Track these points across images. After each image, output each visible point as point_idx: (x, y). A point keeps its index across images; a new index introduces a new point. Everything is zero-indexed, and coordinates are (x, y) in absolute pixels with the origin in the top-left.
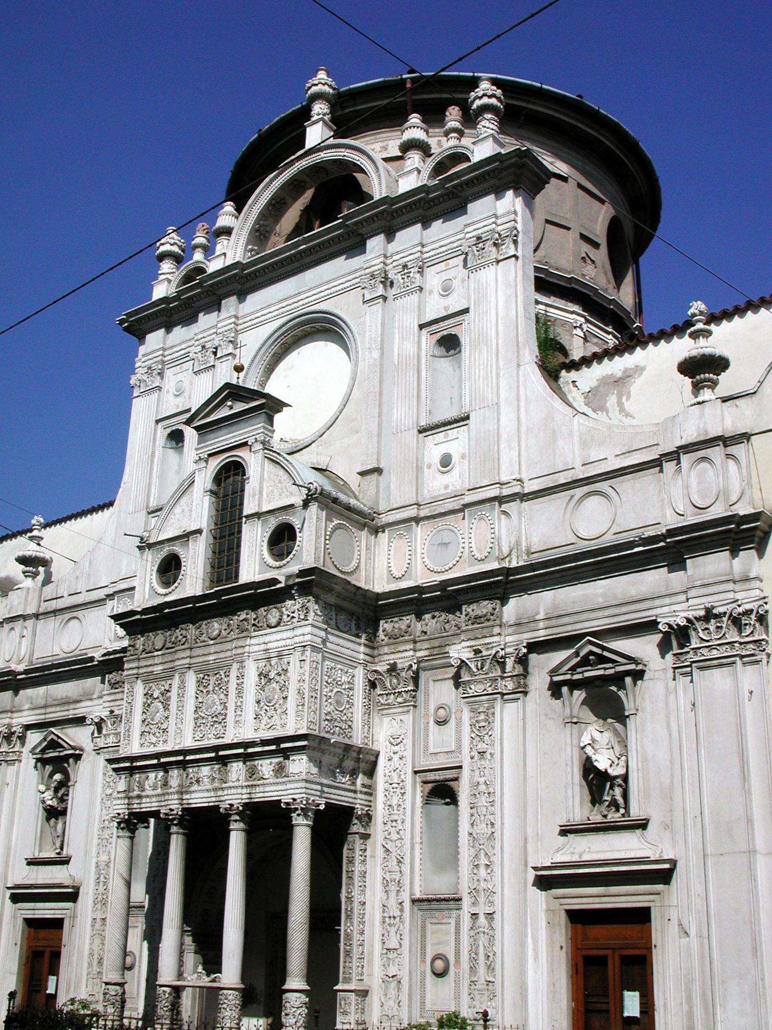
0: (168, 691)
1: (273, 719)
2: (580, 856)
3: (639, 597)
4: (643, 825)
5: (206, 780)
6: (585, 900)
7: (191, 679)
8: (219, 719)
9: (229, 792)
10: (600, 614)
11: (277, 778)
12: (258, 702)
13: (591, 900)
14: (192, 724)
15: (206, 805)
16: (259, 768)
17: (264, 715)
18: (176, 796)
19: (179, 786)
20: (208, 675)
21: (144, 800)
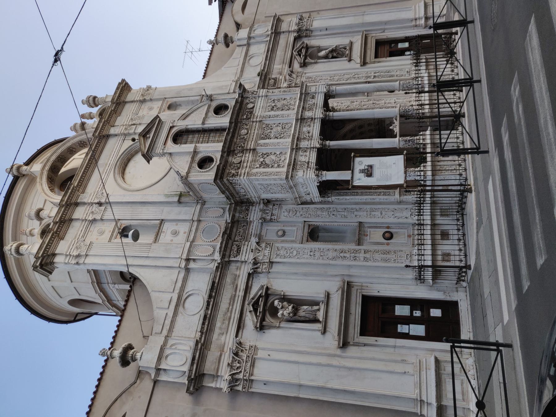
0: (263, 153)
5: (309, 129)
12: (282, 110)
15: (320, 125)
16: (310, 105)
18: (313, 141)
19: (308, 141)
21: (310, 161)
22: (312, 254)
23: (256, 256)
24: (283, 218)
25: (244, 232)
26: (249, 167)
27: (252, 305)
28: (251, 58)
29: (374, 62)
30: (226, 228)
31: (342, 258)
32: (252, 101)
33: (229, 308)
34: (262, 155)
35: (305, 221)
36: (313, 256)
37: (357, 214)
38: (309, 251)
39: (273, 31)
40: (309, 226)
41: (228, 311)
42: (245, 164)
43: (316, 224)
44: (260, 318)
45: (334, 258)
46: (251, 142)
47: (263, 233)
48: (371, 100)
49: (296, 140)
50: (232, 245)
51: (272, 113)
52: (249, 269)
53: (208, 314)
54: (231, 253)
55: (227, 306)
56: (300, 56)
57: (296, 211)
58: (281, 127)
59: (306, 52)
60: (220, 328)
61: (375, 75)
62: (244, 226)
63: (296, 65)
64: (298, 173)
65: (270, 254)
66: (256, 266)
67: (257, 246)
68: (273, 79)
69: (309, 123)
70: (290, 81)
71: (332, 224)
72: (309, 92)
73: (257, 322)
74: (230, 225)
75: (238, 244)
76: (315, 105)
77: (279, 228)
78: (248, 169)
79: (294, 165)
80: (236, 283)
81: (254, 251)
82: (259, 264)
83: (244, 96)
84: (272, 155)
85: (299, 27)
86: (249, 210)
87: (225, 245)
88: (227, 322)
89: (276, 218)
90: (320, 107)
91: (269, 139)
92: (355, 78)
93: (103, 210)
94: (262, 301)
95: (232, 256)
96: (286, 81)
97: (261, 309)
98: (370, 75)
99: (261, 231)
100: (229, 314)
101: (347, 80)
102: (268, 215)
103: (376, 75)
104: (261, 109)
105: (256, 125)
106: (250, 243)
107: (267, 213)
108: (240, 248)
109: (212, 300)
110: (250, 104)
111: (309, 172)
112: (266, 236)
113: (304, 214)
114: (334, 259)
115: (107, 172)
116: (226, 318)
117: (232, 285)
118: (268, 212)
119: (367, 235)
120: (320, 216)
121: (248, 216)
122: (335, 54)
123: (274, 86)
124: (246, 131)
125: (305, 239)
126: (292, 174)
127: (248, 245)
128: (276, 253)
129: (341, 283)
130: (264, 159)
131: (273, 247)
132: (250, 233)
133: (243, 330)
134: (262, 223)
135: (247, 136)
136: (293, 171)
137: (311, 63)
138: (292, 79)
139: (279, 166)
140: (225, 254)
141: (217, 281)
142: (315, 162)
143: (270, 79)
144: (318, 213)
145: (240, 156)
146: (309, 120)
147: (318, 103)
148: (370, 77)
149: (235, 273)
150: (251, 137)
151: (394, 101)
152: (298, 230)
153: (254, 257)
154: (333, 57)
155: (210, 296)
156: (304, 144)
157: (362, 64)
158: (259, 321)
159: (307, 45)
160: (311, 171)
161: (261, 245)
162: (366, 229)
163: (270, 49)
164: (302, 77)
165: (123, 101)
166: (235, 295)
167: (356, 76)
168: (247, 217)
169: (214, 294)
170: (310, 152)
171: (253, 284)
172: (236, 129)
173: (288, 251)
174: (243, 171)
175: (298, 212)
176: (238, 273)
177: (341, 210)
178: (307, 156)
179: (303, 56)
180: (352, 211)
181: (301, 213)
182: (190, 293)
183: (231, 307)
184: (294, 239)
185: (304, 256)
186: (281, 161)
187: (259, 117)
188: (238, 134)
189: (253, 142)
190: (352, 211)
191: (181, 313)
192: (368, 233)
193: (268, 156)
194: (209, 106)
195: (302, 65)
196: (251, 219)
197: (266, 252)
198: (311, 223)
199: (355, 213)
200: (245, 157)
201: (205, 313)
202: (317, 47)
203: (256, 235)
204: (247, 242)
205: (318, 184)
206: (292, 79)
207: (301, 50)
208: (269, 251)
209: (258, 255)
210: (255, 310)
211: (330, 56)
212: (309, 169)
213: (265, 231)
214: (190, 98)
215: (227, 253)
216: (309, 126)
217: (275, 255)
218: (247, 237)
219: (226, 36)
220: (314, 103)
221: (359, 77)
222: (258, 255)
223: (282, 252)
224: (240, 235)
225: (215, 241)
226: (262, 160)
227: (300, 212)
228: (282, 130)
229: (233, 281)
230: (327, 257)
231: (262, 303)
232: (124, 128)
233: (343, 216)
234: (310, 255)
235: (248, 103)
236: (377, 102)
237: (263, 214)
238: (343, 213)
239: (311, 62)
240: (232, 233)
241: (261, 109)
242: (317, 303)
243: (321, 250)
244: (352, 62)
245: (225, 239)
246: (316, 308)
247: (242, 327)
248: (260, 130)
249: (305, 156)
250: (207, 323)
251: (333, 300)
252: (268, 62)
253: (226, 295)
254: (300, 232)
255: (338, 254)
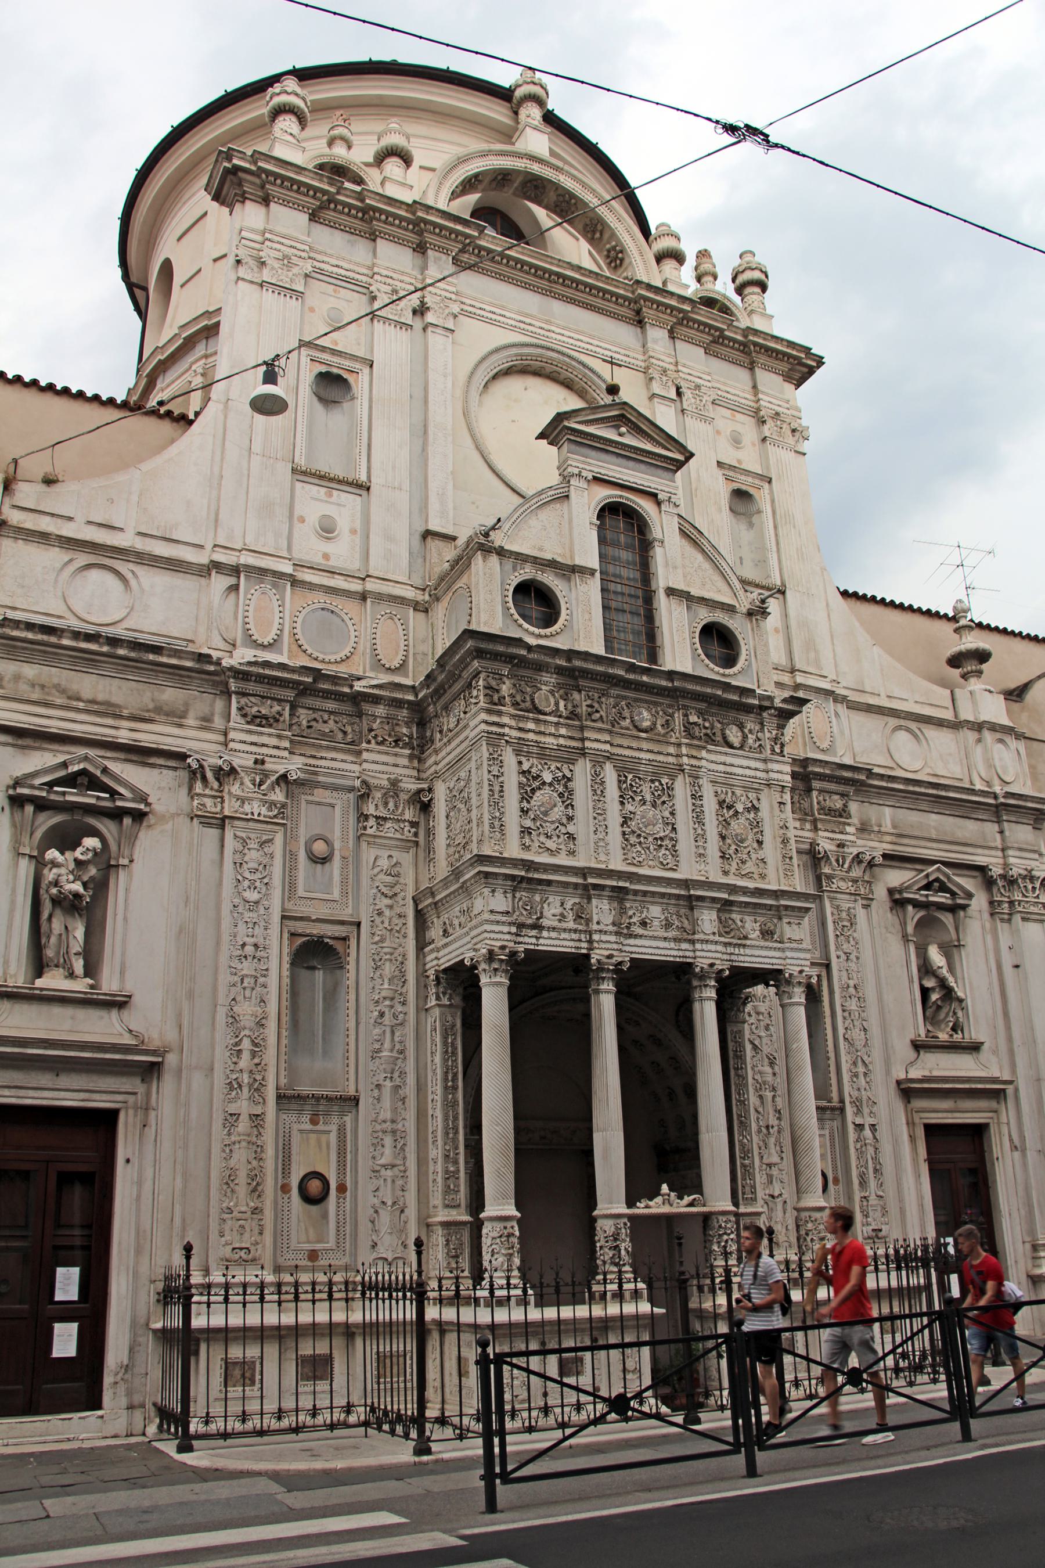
0: (569, 780)
1: (748, 864)
2: (930, 1071)
3: (963, 841)
4: (975, 1048)
5: (656, 923)
6: (940, 1115)
7: (610, 774)
8: (667, 842)
9: (705, 947)
10: (935, 845)
11: (766, 940)
12: (723, 838)
13: (945, 1115)
14: (619, 838)
15: (672, 959)
16: (739, 923)
17: (734, 856)
18: (613, 938)
19: (614, 924)
20: (640, 778)
21: (545, 934)
22: (249, 949)
23: (242, 774)
24: (369, 854)
25: (324, 734)
26: (520, 738)
27: (84, 769)
28: (916, 736)
29: (910, 1124)
30: (334, 679)
31: (237, 1044)
32: (750, 741)
33: (79, 699)
34: (564, 776)
35: (359, 924)
36: (239, 952)
37: (383, 1090)
38: (260, 941)
39: (1002, 800)
40: (345, 939)
41: (69, 698)
42: (531, 726)
43: (352, 959)
44: (44, 794)
45: (234, 1019)
46: (606, 742)
47: (320, 795)
48: (779, 1119)
49: (614, 883)
50: (280, 701)
51: (710, 805)
52: (198, 756)
53: (60, 637)
54: (252, 699)
55: (87, 694)
56: (928, 887)
57: (396, 894)
58: (662, 834)
59: (940, 907)
60: (17, 678)
61: (867, 1127)
62: (345, 733)
63: (896, 877)
64: (499, 894)
65: (249, 816)
66: (209, 775)
67: (273, 778)
68: (845, 806)
69: (677, 923)
70: (837, 861)
71: (352, 1012)
72: (785, 920)
73: (33, 787)
74: (347, 690)
75: (282, 719)
76: (739, 942)
77: (337, 845)
78: (515, 733)
79: (530, 880)
80: (157, 718)
81: (259, 767)
82: (216, 785)
83: (765, 714)
84: (562, 808)
85: (1020, 881)
86: (397, 745)
87: (277, 678)
88: (35, 696)
89: (369, 831)
90: (733, 957)
91: (621, 796)
92: (855, 1064)
93: (402, 320)
94: (98, 798)
95: (244, 701)
96: (838, 846)
97: (73, 796)
98: (866, 1110)
99: (325, 787)
100: (59, 701)
101: (845, 1039)
102: (381, 808)
103: (867, 1132)
104: (721, 768)
105: (668, 754)
106: (286, 754)
107: (386, 804)
108: (270, 726)
109: (105, 649)
110: (740, 734)
111: (506, 929)
112: (308, 802)
113: (383, 922)
114: (231, 1020)
115: (522, 326)
116: (48, 694)
117: (151, 706)
118: (391, 805)
119: (314, 1122)
120: (378, 973)
121: (377, 743)
122: (934, 997)
123: (818, 810)
124: (646, 724)
125: (300, 927)
126: (496, 874)
127: (278, 748)
128: (252, 836)
129: (155, 1044)
130: (551, 784)
131: (270, 827)
132: (319, 755)
133: (13, 745)
134: (351, 789)
135: (627, 729)
136: (507, 877)
137: (903, 924)
138: (846, 866)
139: (526, 831)
140: (251, 680)
141: (164, 660)
142: (540, 948)
143: (843, 795)
144: (388, 964)
145: (558, 709)
146: (686, 922)
147: (748, 951)
148: (859, 1112)
149: (191, 714)
150: (625, 742)
151: (776, 1194)
152: (329, 905)
153: (239, 769)
154: (925, 992)
155: (114, 642)
156: (602, 911)
157: (903, 1086)
158: (37, 793)
159: (964, 907)
160: (508, 937)
161: (277, 789)
162: (335, 1120)
163: (943, 793)
164: (853, 898)
165: (754, 362)
166: (121, 717)
167: (861, 1069)
168: (373, 741)
169: (121, 652)
170: (575, 931)
171: (156, 771)
172: (652, 693)
173: (258, 875)
174: (506, 720)
175: (388, 901)
176: (190, 721)
177: (397, 1039)
178: (560, 921)
179: (927, 896)
180: (396, 1075)
181: (387, 912)
182: (133, 582)
183: (81, 705)
184: (301, 892)
185: (242, 928)
186: (542, 838)
187: (694, 762)
188: (636, 700)
189: (607, 747)
190: (396, 1075)
191: (71, 560)
192: (321, 1127)
193: (561, 795)
194: (730, 609)
195: (897, 896)
196: (365, 755)
197: (256, 804)
198: (353, 943)
199: (388, 1084)
200: (557, 724)
201: (63, 631)
202: (959, 940)
203: (315, 773)
204: (287, 744)
205: (467, 962)
206: (846, 866)
207: (943, 888)
208: (259, 814)
209: (247, 781)
210: (70, 781)
211: (930, 983)
212: (514, 930)
213: (328, 801)
214: (775, 556)
215: (251, 687)
216: (668, 925)
217: (244, 835)
218: (306, 744)
219: (982, 656)
220: (746, 938)
221: (856, 1075)
222: (247, 781)
223: (253, 856)
224: (313, 723)
225: (295, 647)
226: (547, 777)
227: (391, 907)
228: (650, 839)
229: (165, 708)
230: (240, 998)
231: (93, 801)
232: (667, 366)
233: (377, 1046)
234: (244, 945)
235: (741, 727)
236: (772, 1140)
237: (383, 791)
238: (387, 1045)
239: (905, 923)
240: (318, 696)
241: (721, 768)
242: (91, 970)
243: (261, 980)
244: (912, 1054)
245: (296, 677)
246: (79, 965)
247: (20, 742)
248: (650, 769)
249: (562, 915)
250: (30, 636)
251: (102, 1018)
252: (901, 787)
253: (120, 688)
254: (323, 911)
255: (247, 1032)
